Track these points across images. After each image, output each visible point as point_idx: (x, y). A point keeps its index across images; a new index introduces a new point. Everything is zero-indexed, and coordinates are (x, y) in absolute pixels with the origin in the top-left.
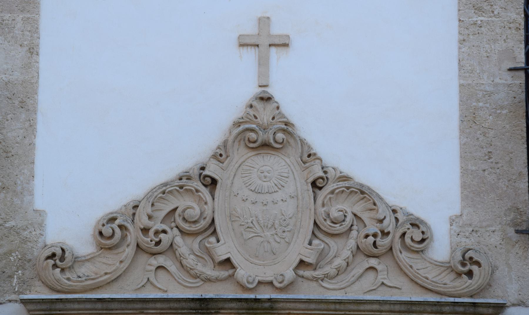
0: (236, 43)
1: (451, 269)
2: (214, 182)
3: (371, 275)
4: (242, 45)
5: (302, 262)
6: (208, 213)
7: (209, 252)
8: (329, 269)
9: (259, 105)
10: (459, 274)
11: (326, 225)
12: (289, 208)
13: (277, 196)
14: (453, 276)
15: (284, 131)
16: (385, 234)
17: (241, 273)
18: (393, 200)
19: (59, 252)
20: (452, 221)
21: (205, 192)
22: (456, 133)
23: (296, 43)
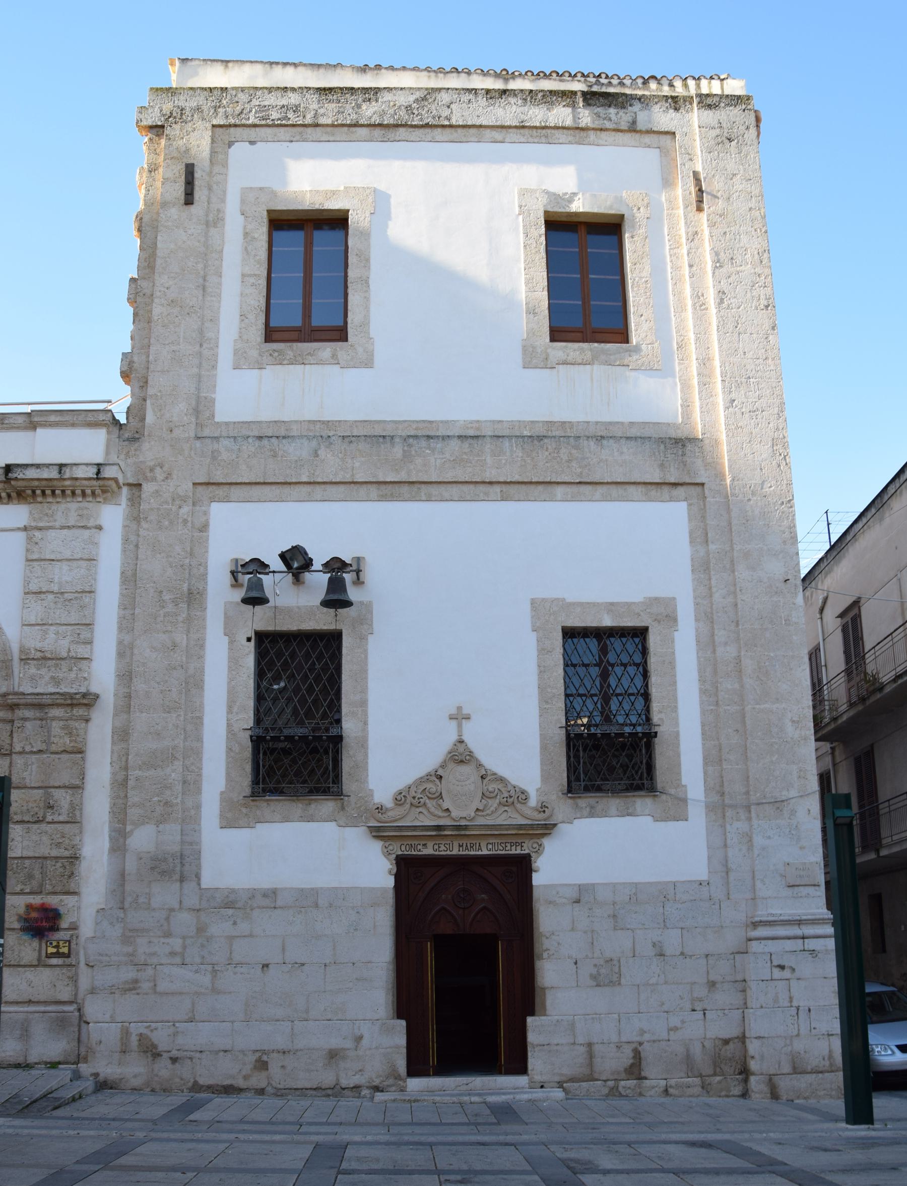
0: (448, 719)
1: (537, 810)
2: (441, 777)
3: (505, 813)
4: (450, 719)
5: (477, 809)
6: (439, 790)
7: (439, 805)
8: (488, 812)
9: (458, 744)
10: (540, 812)
11: (487, 794)
12: (472, 787)
13: (467, 783)
14: (537, 813)
15: (469, 755)
16: (511, 797)
17: (453, 814)
18: (513, 782)
19: (380, 807)
20: (537, 790)
21: (437, 781)
22: (539, 754)
23: (473, 717)
